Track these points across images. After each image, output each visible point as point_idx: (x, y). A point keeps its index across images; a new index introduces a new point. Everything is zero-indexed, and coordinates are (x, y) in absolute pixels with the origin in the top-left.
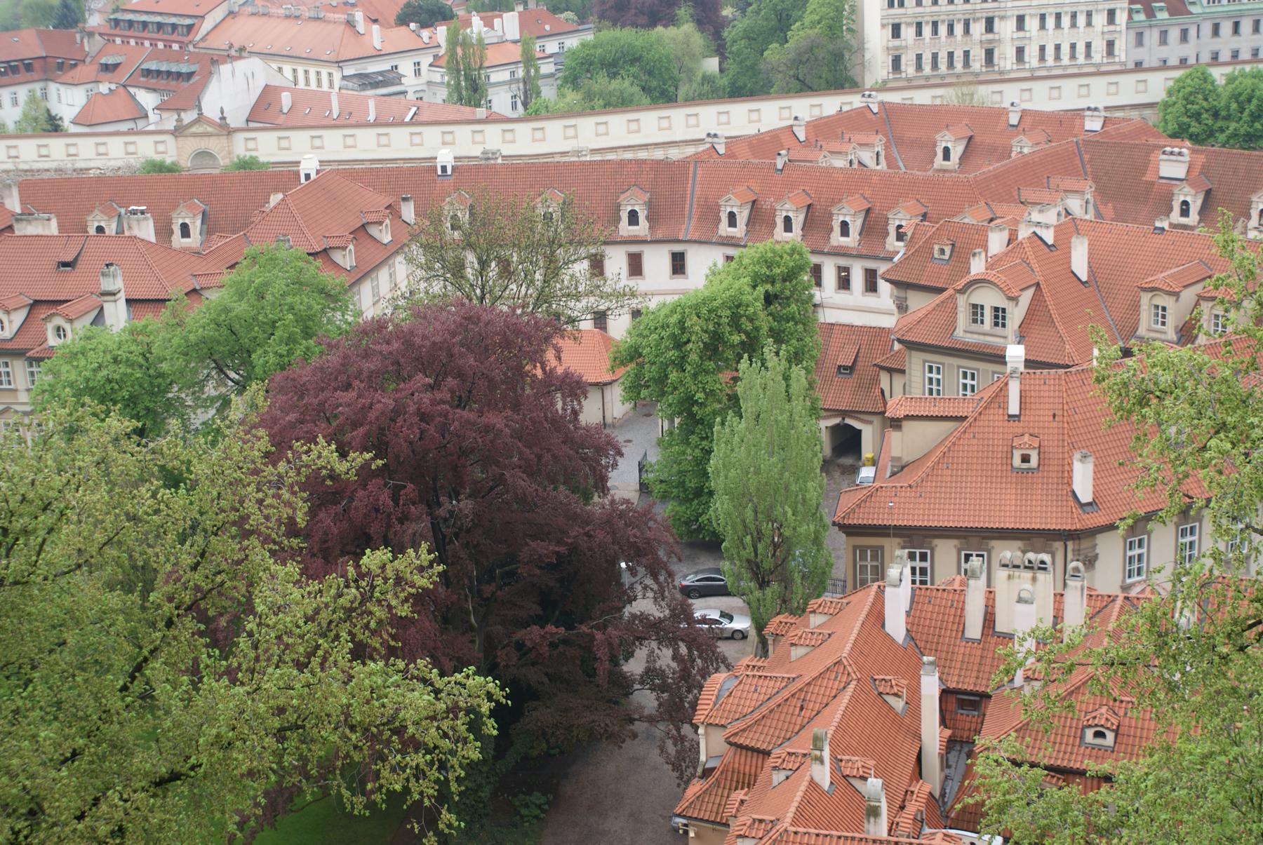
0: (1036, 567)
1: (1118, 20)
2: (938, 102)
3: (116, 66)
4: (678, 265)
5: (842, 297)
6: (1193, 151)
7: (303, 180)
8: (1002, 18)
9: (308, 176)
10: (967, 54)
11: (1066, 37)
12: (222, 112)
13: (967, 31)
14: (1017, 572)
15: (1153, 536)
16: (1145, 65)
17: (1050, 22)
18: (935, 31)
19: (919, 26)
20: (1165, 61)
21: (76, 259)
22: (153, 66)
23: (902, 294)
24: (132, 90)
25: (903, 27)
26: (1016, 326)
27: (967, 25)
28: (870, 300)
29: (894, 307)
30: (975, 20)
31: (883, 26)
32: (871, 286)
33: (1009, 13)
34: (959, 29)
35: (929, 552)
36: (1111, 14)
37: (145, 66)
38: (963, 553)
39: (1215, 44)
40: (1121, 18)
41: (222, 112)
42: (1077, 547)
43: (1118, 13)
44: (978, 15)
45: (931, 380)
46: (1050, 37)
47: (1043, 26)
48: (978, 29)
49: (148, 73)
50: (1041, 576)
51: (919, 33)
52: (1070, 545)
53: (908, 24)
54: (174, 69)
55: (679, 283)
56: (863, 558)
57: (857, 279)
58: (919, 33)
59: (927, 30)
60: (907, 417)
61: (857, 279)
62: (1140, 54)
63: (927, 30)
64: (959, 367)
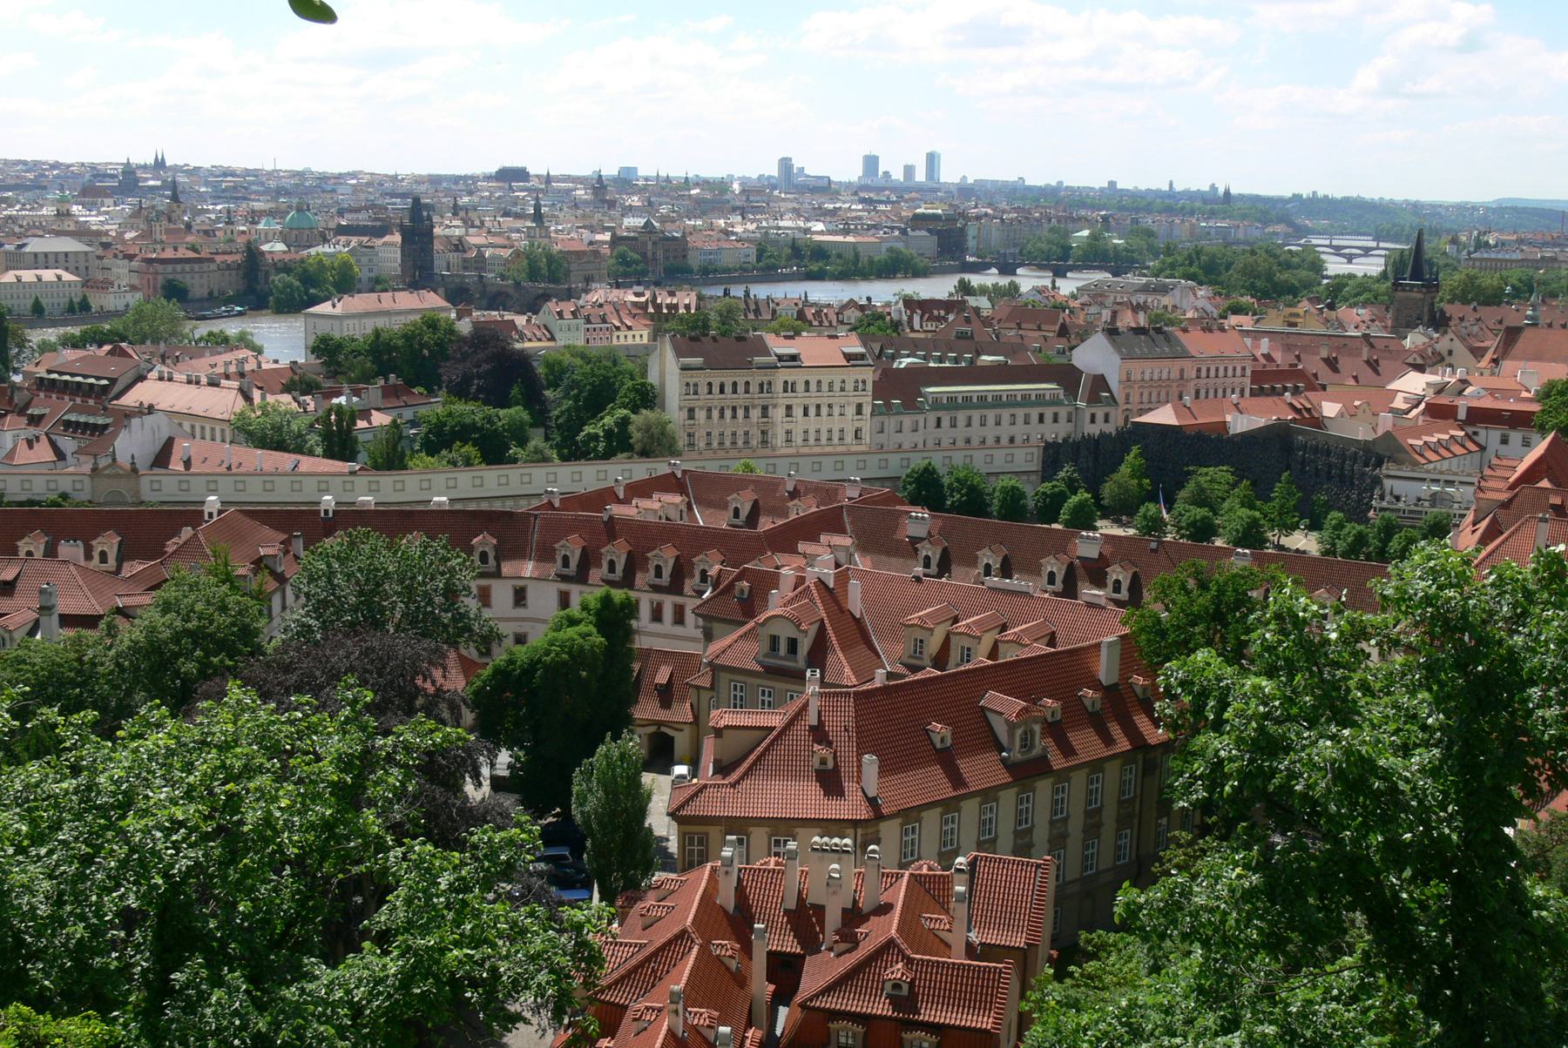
1: (864, 412)
3: (41, 417)
4: (520, 597)
5: (656, 627)
6: (933, 517)
7: (206, 518)
8: (775, 406)
9: (211, 515)
10: (747, 433)
11: (824, 423)
12: (133, 457)
13: (747, 417)
14: (826, 854)
15: (923, 822)
16: (885, 448)
17: (812, 411)
18: (722, 415)
19: (709, 410)
20: (900, 446)
21: (16, 578)
22: (73, 417)
23: (709, 625)
24: (53, 437)
25: (697, 410)
26: (805, 653)
27: (747, 409)
28: (678, 630)
29: (701, 636)
30: (754, 407)
31: (681, 409)
32: (679, 619)
33: (780, 401)
34: (740, 413)
36: (859, 408)
37: (65, 418)
39: (939, 433)
40: (867, 410)
41: (133, 457)
43: (864, 406)
44: (756, 402)
45: (735, 696)
46: (812, 423)
47: (806, 414)
48: (755, 414)
49: (68, 424)
50: (845, 856)
51: (709, 417)
52: (860, 831)
53: (701, 408)
54: (91, 420)
55: (521, 612)
56: (691, 843)
57: (668, 613)
58: (709, 417)
59: (715, 414)
60: (727, 727)
61: (668, 613)
62: (882, 438)
63: (715, 414)
64: (759, 686)
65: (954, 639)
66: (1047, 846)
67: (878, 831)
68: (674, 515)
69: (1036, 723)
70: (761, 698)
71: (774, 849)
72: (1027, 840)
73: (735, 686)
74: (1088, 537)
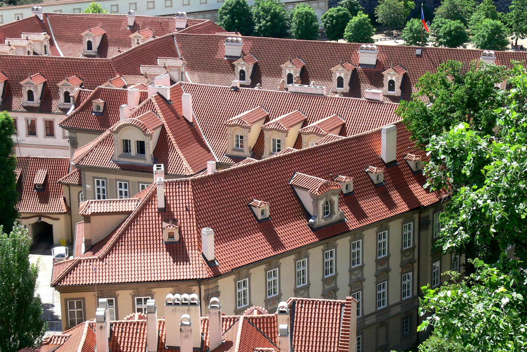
0: (189, 304)
2: (77, 13)
5: (31, 140)
6: (245, 40)
14: (178, 307)
23: (73, 135)
26: (151, 152)
28: (50, 141)
32: (50, 132)
35: (114, 299)
38: (136, 298)
42: (207, 288)
45: (99, 189)
50: (192, 308)
56: (72, 307)
57: (40, 128)
60: (94, 214)
61: (40, 128)
65: (267, 134)
66: (348, 289)
67: (217, 287)
68: (39, 50)
69: (334, 195)
70: (119, 189)
71: (137, 307)
72: (333, 285)
73: (98, 182)
74: (367, 49)
